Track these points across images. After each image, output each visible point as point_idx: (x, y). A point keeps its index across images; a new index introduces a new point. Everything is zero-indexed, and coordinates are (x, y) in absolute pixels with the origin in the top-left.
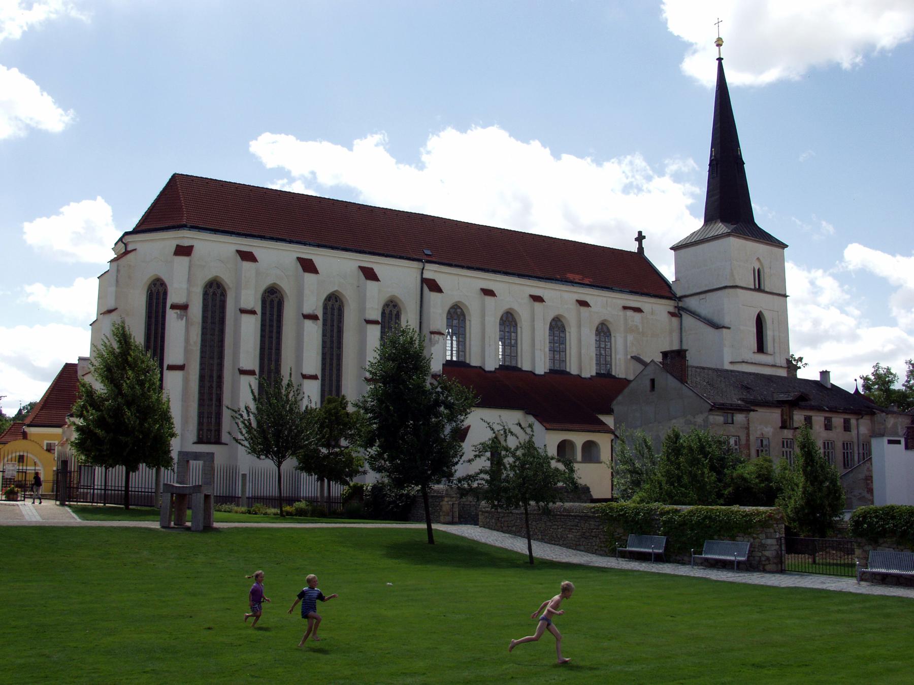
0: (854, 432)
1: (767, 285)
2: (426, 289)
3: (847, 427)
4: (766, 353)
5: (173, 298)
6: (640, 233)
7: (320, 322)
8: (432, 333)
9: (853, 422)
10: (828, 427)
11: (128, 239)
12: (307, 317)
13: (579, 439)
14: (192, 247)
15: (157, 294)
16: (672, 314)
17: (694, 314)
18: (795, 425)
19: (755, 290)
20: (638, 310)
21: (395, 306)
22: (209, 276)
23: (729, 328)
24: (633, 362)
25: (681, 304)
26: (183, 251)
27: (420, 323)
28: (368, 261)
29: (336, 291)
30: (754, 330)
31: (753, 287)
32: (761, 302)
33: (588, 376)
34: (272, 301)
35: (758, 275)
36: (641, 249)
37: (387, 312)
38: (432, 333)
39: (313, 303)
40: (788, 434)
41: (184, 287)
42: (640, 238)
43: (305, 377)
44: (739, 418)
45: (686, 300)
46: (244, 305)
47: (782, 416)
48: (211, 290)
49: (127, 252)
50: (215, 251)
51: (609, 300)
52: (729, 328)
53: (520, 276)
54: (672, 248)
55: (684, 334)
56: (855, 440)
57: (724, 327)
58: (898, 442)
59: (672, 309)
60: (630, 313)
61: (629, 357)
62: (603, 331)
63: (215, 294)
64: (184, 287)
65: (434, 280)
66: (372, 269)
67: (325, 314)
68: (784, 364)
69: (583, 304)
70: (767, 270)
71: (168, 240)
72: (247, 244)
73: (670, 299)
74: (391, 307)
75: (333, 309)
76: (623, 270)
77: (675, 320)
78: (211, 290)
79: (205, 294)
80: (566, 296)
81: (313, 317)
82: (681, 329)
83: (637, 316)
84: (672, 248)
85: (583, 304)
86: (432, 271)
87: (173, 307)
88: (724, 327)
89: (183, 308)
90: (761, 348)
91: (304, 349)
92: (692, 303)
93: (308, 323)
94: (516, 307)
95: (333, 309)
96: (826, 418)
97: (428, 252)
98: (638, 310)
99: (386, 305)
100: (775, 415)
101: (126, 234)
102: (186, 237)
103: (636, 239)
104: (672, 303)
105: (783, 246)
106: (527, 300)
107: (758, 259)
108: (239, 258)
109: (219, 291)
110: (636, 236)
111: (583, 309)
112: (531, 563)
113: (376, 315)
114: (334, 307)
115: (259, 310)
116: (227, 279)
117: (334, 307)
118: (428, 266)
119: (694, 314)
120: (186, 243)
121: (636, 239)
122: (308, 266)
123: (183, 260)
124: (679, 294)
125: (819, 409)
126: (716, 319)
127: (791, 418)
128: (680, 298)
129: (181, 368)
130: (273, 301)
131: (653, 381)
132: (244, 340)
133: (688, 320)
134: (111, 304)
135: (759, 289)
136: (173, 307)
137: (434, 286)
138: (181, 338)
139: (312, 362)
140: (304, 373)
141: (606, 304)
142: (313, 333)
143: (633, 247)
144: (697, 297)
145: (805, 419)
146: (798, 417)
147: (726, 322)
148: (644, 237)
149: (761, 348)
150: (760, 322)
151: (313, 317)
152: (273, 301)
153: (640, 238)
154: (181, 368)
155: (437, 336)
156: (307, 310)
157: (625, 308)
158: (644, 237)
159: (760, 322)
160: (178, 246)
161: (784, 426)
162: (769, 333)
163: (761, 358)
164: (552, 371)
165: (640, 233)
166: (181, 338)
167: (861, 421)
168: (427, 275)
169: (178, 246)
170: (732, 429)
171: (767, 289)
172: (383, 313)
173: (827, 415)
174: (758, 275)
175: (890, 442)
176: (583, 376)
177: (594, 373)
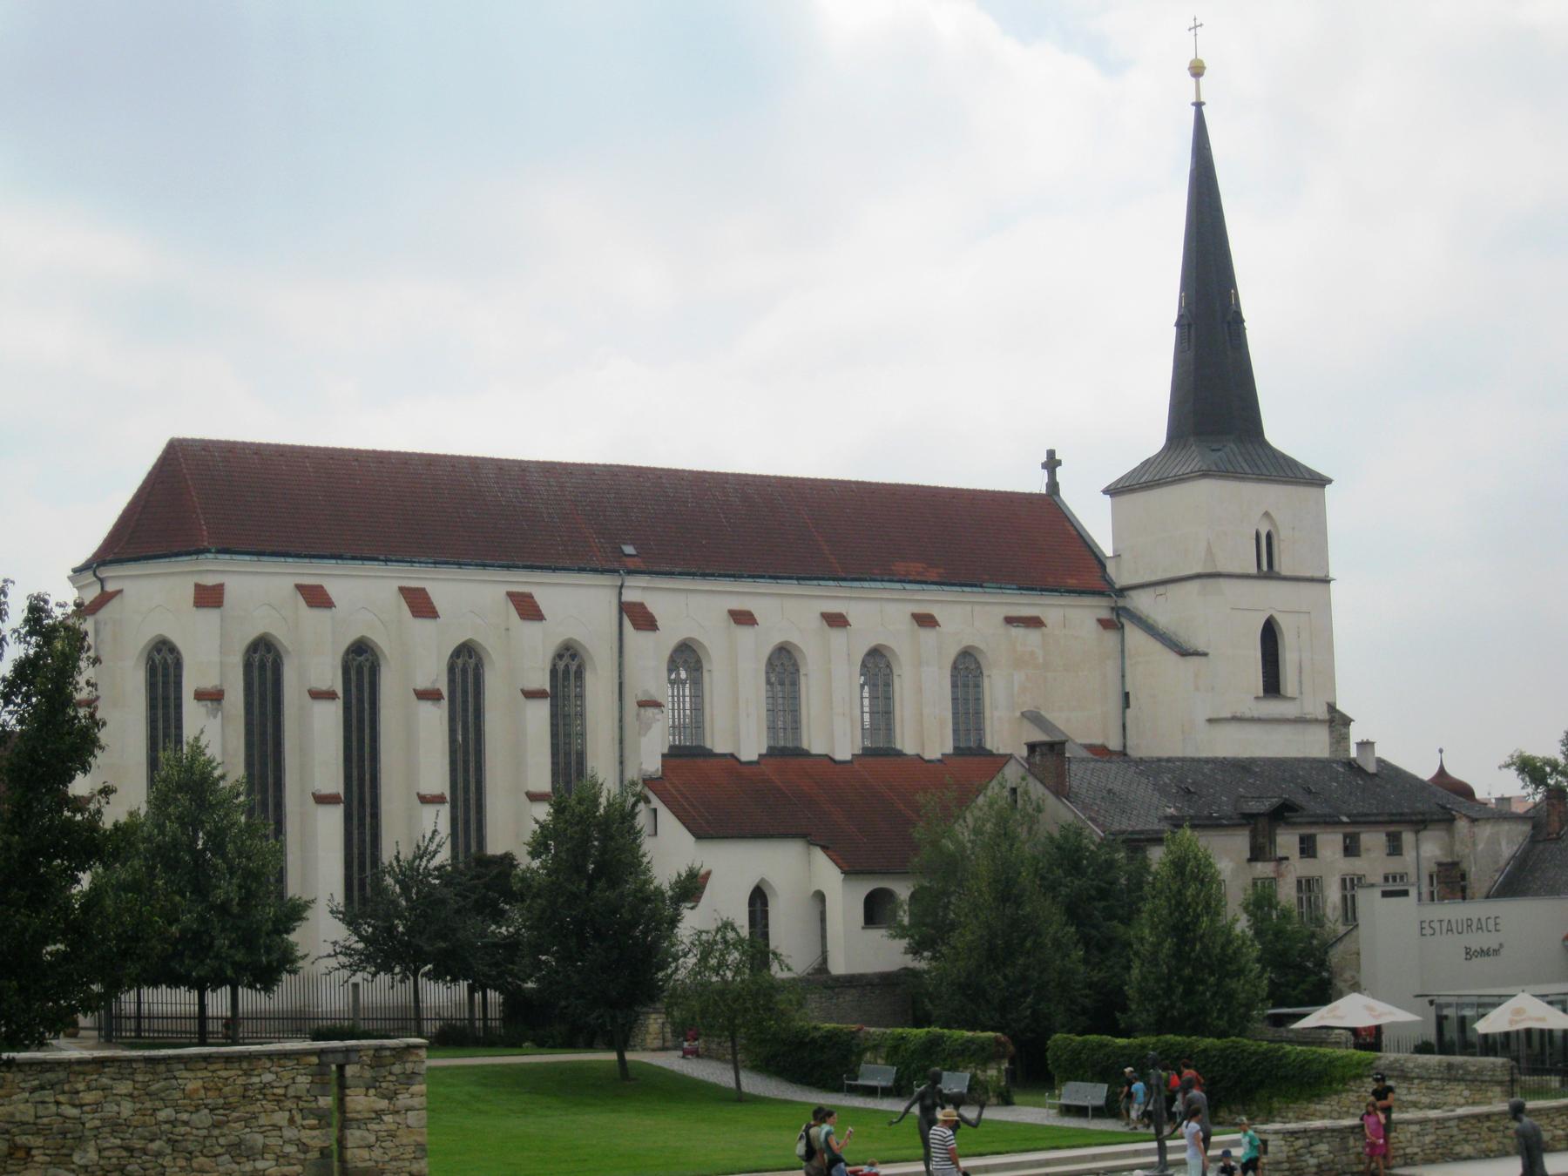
0: (1409, 854)
2: (627, 623)
3: (1395, 848)
4: (1285, 698)
6: (1051, 454)
7: (445, 703)
8: (643, 704)
9: (1408, 837)
10: (1351, 849)
11: (105, 572)
12: (423, 695)
14: (219, 588)
16: (1105, 624)
18: (1280, 853)
20: (1035, 622)
21: (573, 656)
23: (1205, 654)
25: (1121, 603)
27: (621, 685)
28: (522, 581)
29: (470, 640)
31: (1253, 570)
33: (938, 756)
35: (1266, 545)
36: (1053, 486)
37: (561, 665)
38: (643, 704)
39: (433, 671)
40: (1264, 869)
42: (1052, 463)
43: (424, 800)
45: (1133, 594)
47: (1254, 837)
48: (257, 657)
49: (105, 599)
51: (977, 608)
52: (1205, 654)
54: (1106, 492)
55: (1128, 662)
56: (1412, 870)
57: (1196, 654)
58: (1405, 893)
59: (1105, 614)
60: (1018, 632)
61: (1018, 714)
62: (967, 671)
63: (264, 664)
65: (641, 605)
66: (530, 596)
67: (452, 681)
68: (1322, 713)
74: (566, 659)
75: (464, 671)
77: (1111, 637)
78: (257, 657)
79: (248, 666)
80: (891, 608)
82: (1123, 651)
83: (1032, 637)
84: (1106, 492)
86: (638, 590)
87: (200, 696)
88: (1196, 654)
90: (1272, 685)
91: (417, 749)
92: (1141, 602)
94: (794, 638)
95: (464, 671)
96: (1345, 836)
97: (629, 550)
98: (1035, 622)
99: (559, 656)
100: (1240, 842)
103: (1044, 466)
104: (1104, 602)
105: (1320, 481)
106: (817, 623)
107: (1267, 514)
108: (302, 603)
109: (270, 657)
110: (1044, 458)
112: (738, 1097)
113: (541, 680)
115: (340, 693)
116: (282, 635)
117: (467, 666)
118: (631, 581)
120: (210, 581)
121: (1044, 466)
123: (211, 616)
125: (1330, 822)
127: (1273, 842)
128: (1122, 592)
130: (361, 665)
132: (315, 745)
133: (1134, 635)
135: (1268, 571)
136: (200, 696)
137: (644, 620)
139: (435, 776)
140: (423, 792)
141: (971, 617)
142: (433, 722)
143: (1036, 484)
144: (1150, 591)
145: (1302, 840)
146: (1287, 841)
148: (1059, 463)
149: (1272, 685)
150: (1270, 635)
152: (361, 665)
153: (1052, 463)
155: (650, 712)
156: (423, 683)
157: (1010, 621)
158: (1059, 463)
159: (1270, 635)
160: (197, 586)
161: (1250, 860)
163: (1273, 708)
164: (868, 753)
165: (1051, 454)
167: (1424, 834)
168: (630, 596)
169: (197, 586)
171: (1285, 572)
172: (554, 672)
173: (1349, 830)
174: (1266, 545)
175: (1386, 894)
176: (927, 756)
177: (949, 748)
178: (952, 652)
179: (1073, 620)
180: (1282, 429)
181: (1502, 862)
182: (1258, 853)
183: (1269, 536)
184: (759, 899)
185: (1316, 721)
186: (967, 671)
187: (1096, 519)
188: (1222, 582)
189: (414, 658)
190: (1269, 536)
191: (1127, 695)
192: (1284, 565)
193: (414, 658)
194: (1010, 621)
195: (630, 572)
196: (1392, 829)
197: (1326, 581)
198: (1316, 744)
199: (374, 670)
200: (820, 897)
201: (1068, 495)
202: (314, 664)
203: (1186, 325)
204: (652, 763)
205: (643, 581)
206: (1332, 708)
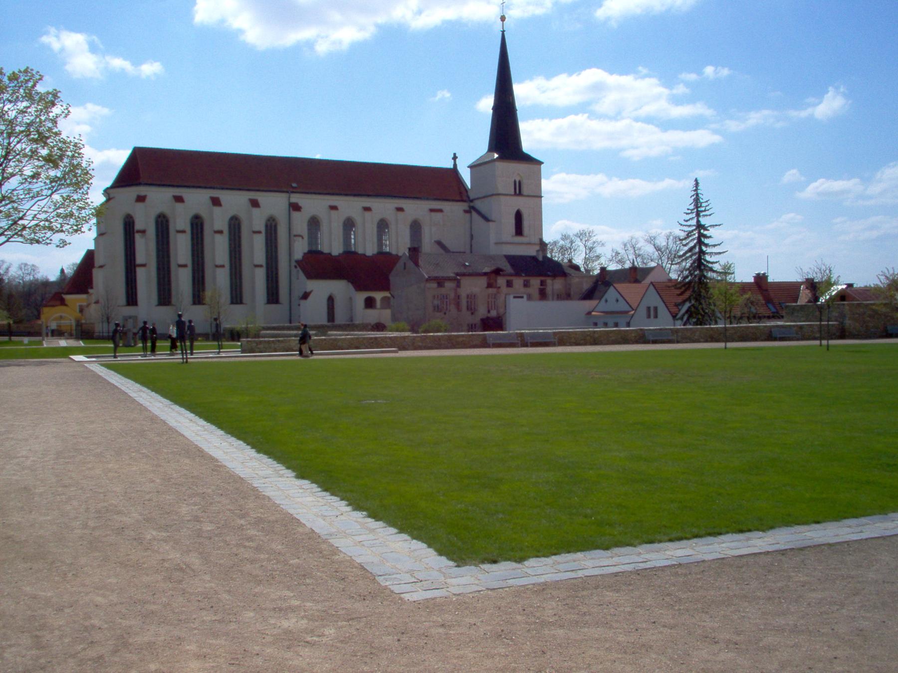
1: (527, 190)
5: (138, 226)
6: (455, 154)
13: (378, 296)
15: (129, 225)
16: (466, 211)
17: (479, 213)
19: (515, 194)
20: (440, 211)
21: (274, 220)
22: (158, 211)
24: (437, 246)
25: (472, 204)
26: (141, 199)
30: (513, 221)
31: (512, 192)
34: (197, 224)
36: (455, 165)
40: (491, 290)
41: (144, 220)
42: (455, 158)
43: (217, 266)
44: (449, 285)
46: (179, 228)
50: (159, 198)
53: (355, 195)
58: (522, 297)
59: (467, 208)
60: (433, 214)
62: (416, 228)
64: (144, 220)
68: (537, 241)
69: (400, 209)
70: (524, 182)
71: (132, 192)
72: (178, 192)
73: (464, 201)
76: (437, 184)
77: (468, 215)
81: (221, 232)
83: (439, 215)
85: (400, 209)
86: (295, 198)
89: (143, 232)
90: (519, 231)
91: (218, 249)
92: (478, 204)
93: (218, 236)
97: (294, 185)
98: (440, 211)
99: (268, 220)
100: (483, 281)
101: (108, 189)
102: (142, 190)
105: (540, 163)
111: (400, 213)
114: (235, 225)
116: (167, 212)
118: (293, 195)
119: (479, 213)
120: (143, 194)
122: (216, 202)
123: (140, 205)
124: (471, 198)
126: (488, 215)
127: (496, 281)
128: (472, 201)
129: (144, 265)
131: (405, 264)
133: (474, 214)
134: (103, 230)
135: (520, 194)
137: (296, 207)
138: (146, 249)
141: (416, 209)
143: (449, 165)
145: (508, 281)
147: (493, 218)
149: (519, 231)
150: (519, 216)
151: (221, 232)
153: (455, 158)
154: (144, 265)
156: (216, 228)
157: (432, 210)
159: (519, 216)
162: (526, 224)
163: (519, 239)
165: (455, 154)
166: (146, 249)
170: (443, 291)
175: (515, 297)
179: (454, 210)
180: (527, 145)
181: (584, 290)
182: (489, 286)
183: (520, 183)
184: (331, 300)
185: (535, 244)
186: (416, 228)
187: (466, 175)
188: (502, 197)
189: (218, 220)
190: (520, 183)
191: (472, 237)
192: (525, 191)
193: (218, 220)
194: (432, 210)
195: (293, 192)
196: (543, 278)
197: (541, 197)
198: (531, 251)
199: (202, 225)
200: (351, 299)
201: (459, 168)
202: (181, 221)
204: (298, 255)
205: (298, 195)
206: (541, 240)
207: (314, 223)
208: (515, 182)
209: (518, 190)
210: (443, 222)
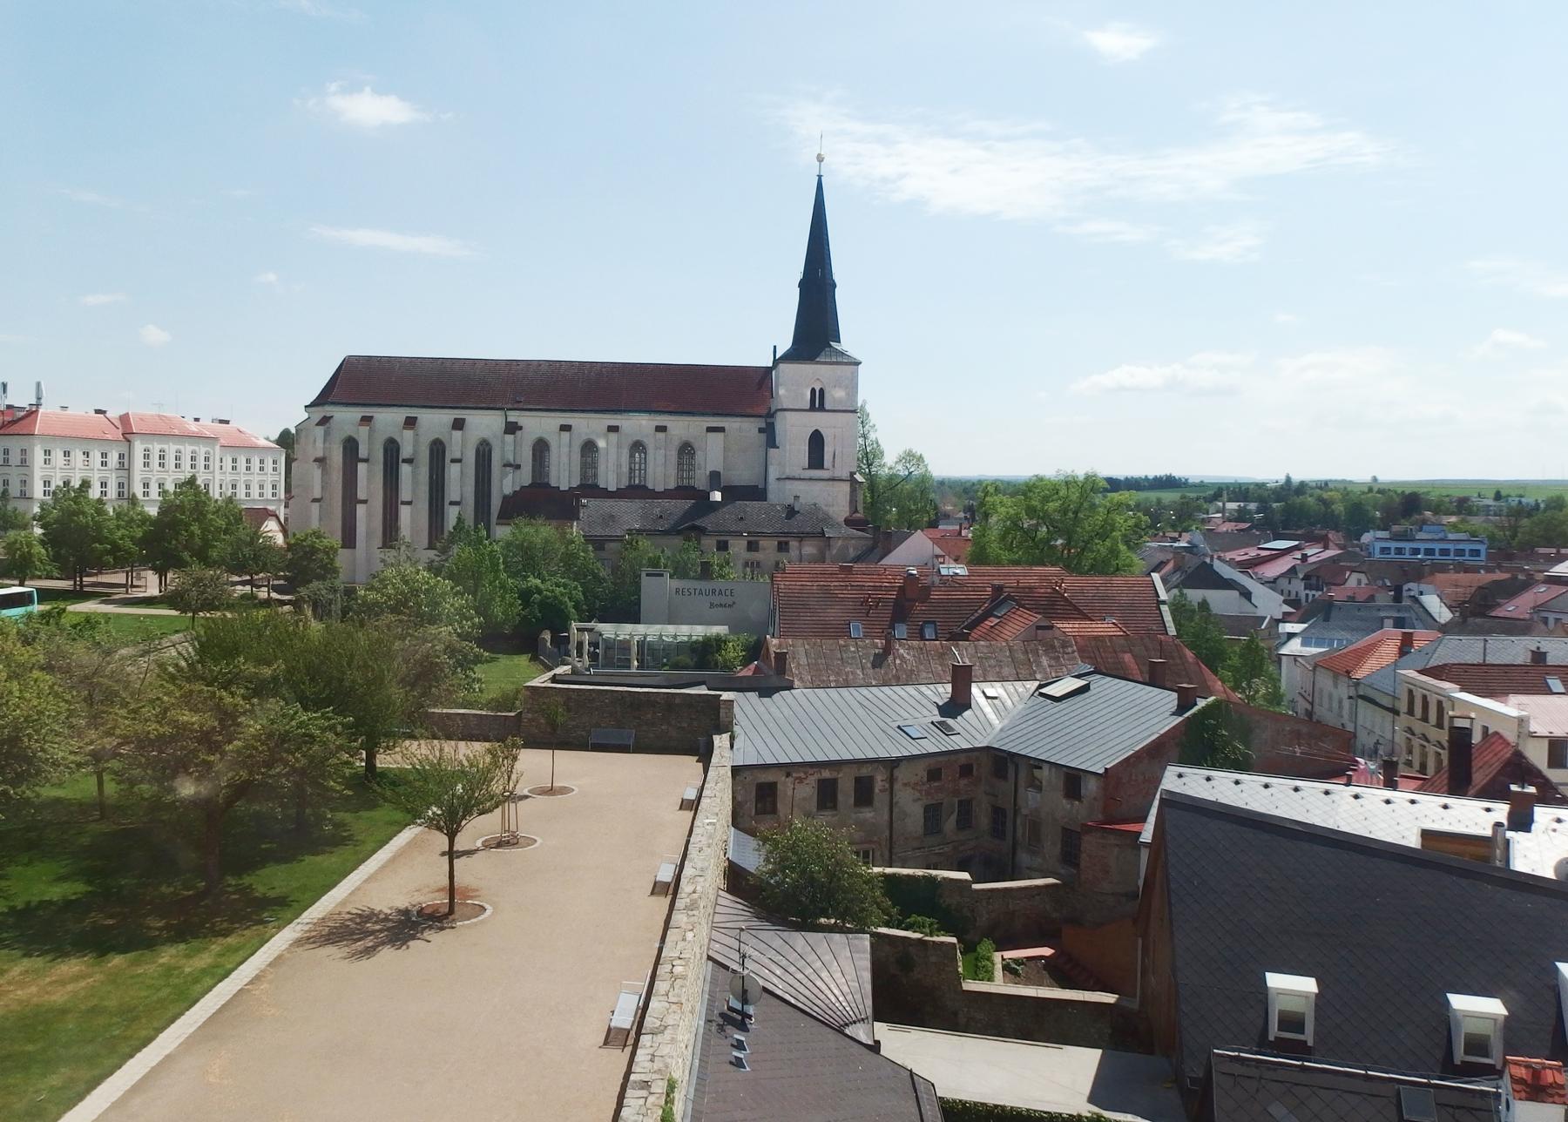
19: (812, 408)
20: (722, 430)
32: (818, 421)
62: (686, 450)
71: (320, 413)
83: (720, 435)
86: (513, 416)
98: (722, 430)
135: (822, 408)
137: (512, 428)
150: (816, 441)
157: (710, 429)
159: (816, 441)
178: (676, 443)
183: (822, 391)
186: (686, 450)
190: (822, 391)
192: (827, 406)
194: (710, 429)
203: (803, 285)
207: (541, 448)
208: (813, 391)
209: (818, 402)
210: (721, 447)
